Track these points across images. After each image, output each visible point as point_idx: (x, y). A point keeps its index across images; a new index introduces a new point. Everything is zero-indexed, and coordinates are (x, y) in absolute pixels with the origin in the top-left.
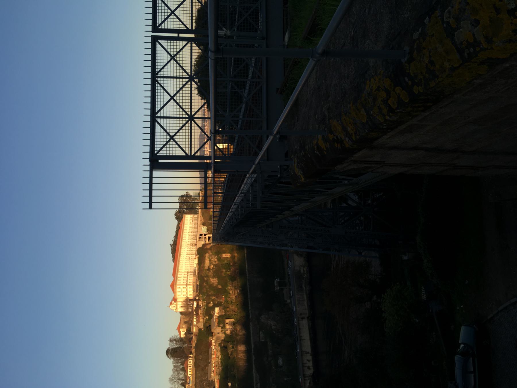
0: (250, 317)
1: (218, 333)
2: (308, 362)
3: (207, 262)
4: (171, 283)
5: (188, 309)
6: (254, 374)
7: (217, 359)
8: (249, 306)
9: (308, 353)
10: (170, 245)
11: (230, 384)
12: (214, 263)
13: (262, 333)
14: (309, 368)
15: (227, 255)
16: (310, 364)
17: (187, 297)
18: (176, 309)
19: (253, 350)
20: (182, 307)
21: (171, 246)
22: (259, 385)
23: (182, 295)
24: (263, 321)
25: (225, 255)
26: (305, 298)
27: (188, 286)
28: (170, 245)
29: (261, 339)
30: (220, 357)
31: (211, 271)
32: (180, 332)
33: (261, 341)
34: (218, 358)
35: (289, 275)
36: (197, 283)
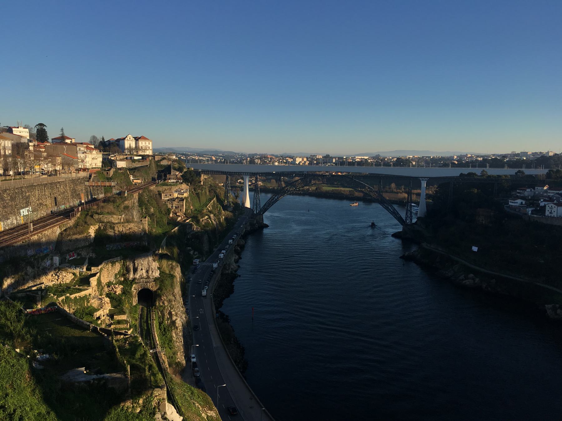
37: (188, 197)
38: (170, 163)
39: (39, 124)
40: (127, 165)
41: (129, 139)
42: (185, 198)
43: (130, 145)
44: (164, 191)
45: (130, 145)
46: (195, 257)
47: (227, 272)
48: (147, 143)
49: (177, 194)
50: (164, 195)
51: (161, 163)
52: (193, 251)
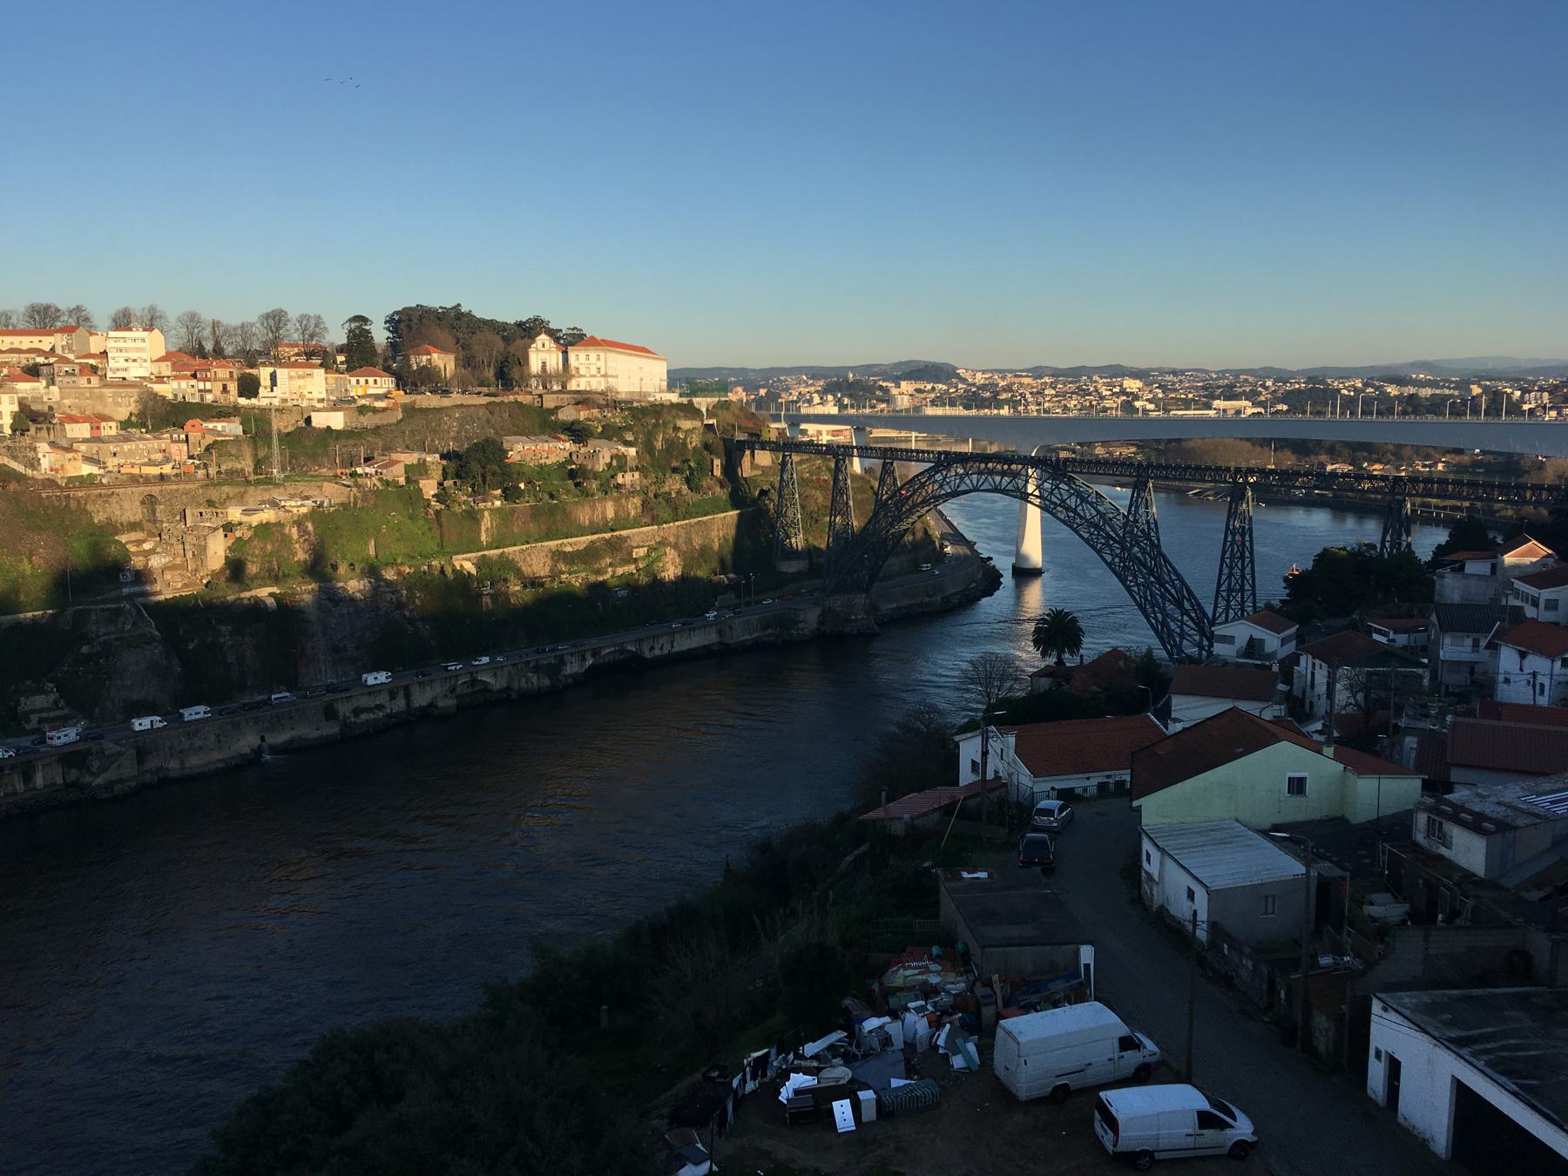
0: (665, 525)
2: (660, 645)
4: (647, 347)
9: (672, 647)
12: (689, 440)
14: (652, 648)
16: (657, 652)
18: (536, 348)
21: (454, 308)
23: (577, 366)
26: (754, 636)
27: (602, 379)
28: (459, 305)
29: (637, 550)
30: (549, 462)
34: (547, 458)
35: (760, 602)
36: (637, 402)
37: (279, 524)
38: (583, 415)
39: (355, 317)
40: (346, 423)
41: (540, 345)
42: (265, 527)
43: (544, 364)
44: (225, 500)
45: (544, 364)
46: (45, 715)
47: (88, 779)
48: (593, 355)
49: (241, 511)
50: (193, 514)
51: (559, 414)
52: (52, 697)
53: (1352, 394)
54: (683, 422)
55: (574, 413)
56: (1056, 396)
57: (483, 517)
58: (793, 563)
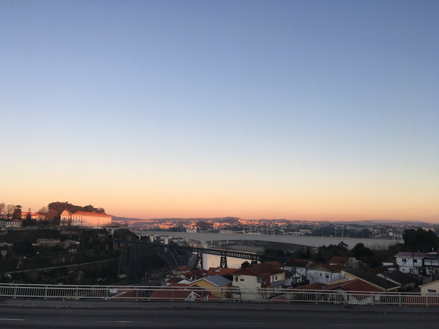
0: (81, 264)
1: (67, 245)
3: (101, 235)
5: (62, 222)
6: (52, 268)
7: (50, 244)
8: (86, 263)
10: (67, 202)
11: (38, 253)
12: (101, 240)
13: (72, 272)
15: (107, 248)
17: (72, 222)
19: (64, 266)
20: (64, 218)
21: (66, 202)
22: (46, 271)
24: (80, 272)
25: (107, 247)
28: (67, 202)
29: (70, 271)
31: (96, 238)
32: (36, 216)
33: (69, 271)
53: (337, 229)
54: (99, 235)
55: (65, 232)
56: (258, 227)
57: (19, 261)
58: (123, 275)
